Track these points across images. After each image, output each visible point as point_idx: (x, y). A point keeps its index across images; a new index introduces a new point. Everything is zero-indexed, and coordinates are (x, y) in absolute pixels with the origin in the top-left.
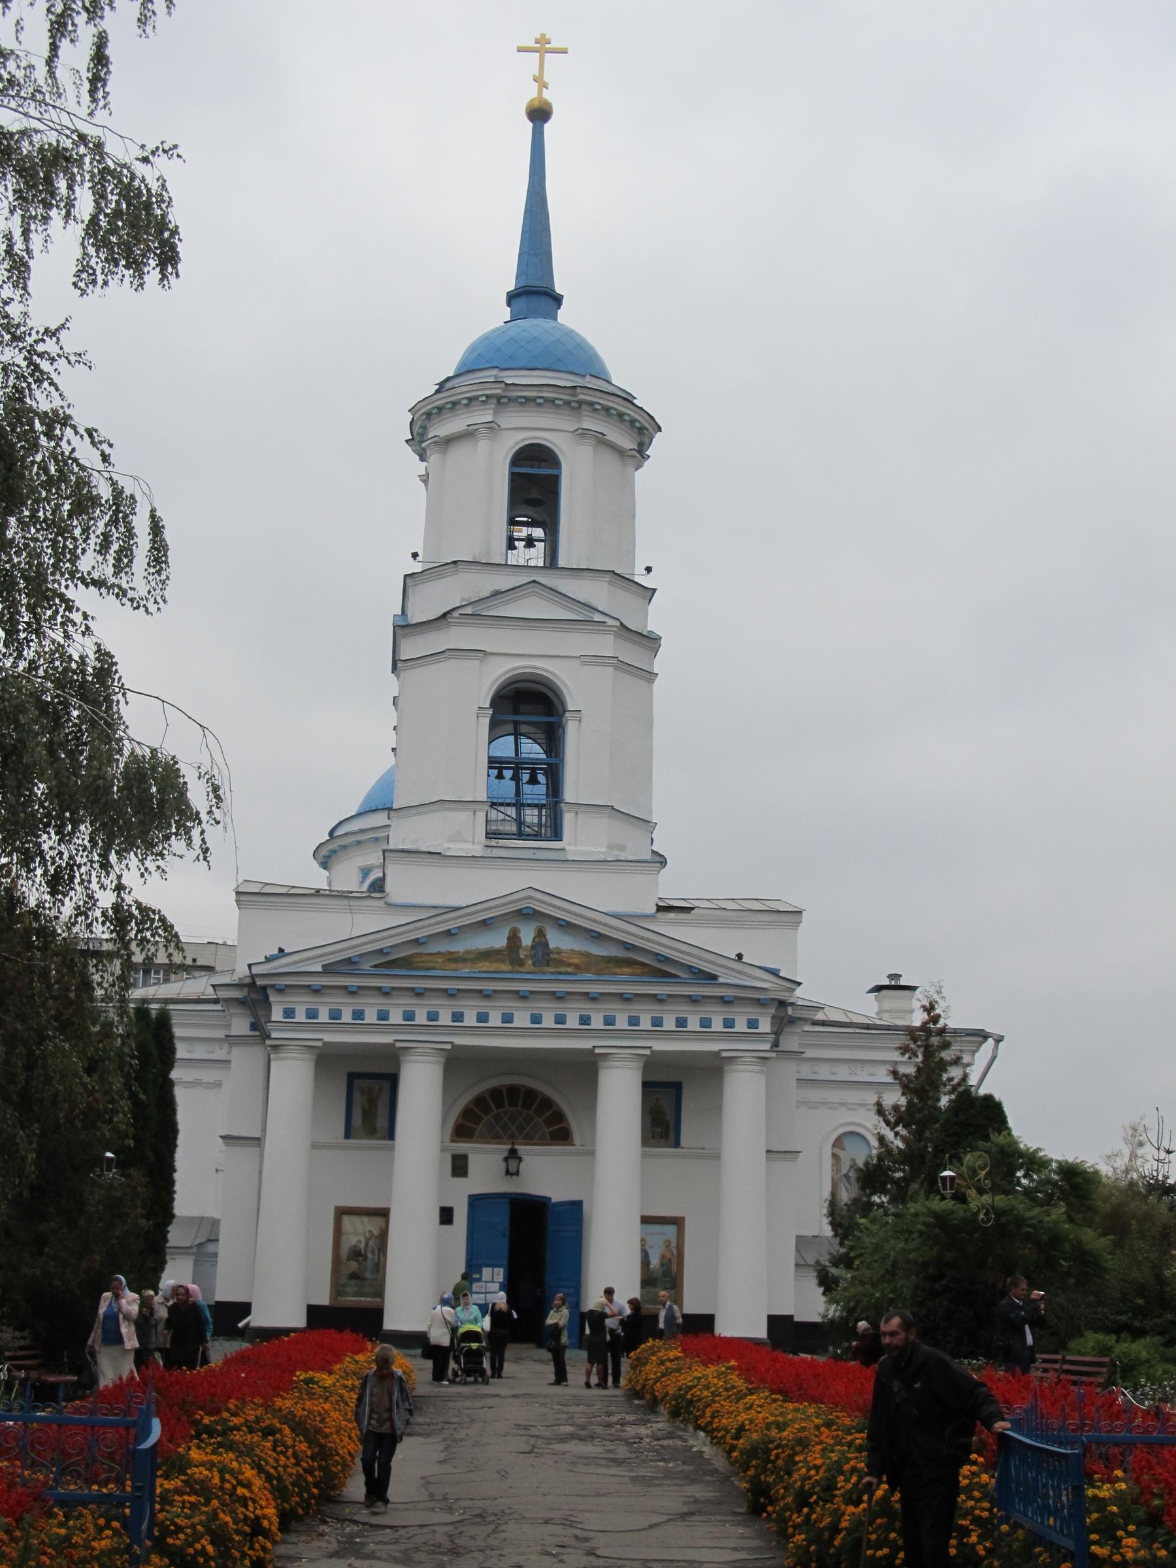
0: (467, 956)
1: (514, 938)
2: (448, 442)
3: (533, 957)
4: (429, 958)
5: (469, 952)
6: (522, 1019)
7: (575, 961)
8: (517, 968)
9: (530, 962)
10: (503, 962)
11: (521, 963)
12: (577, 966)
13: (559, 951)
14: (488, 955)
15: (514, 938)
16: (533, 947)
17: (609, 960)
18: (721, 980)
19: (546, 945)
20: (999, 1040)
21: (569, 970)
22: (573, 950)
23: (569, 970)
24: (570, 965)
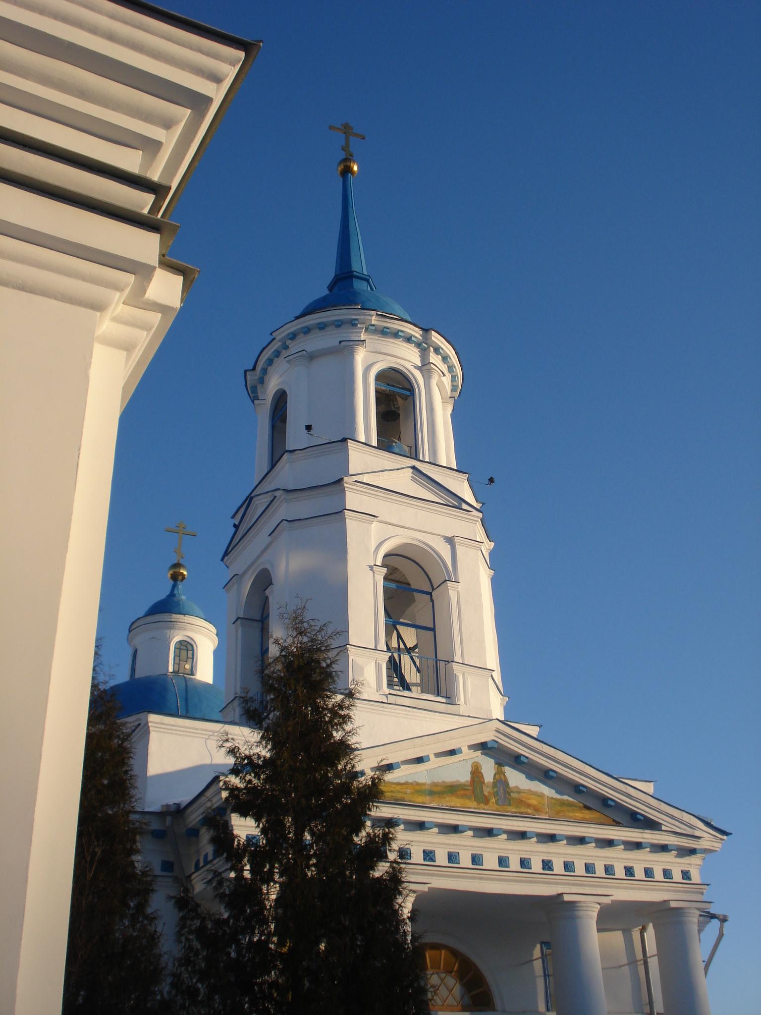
0: (435, 789)
1: (476, 773)
2: (312, 357)
3: (496, 794)
4: (398, 788)
5: (435, 784)
6: (490, 861)
7: (534, 802)
8: (482, 805)
9: (493, 800)
10: (469, 798)
11: (487, 802)
12: (537, 809)
13: (519, 791)
14: (452, 789)
15: (476, 773)
16: (495, 784)
17: (563, 803)
18: (664, 828)
19: (505, 783)
20: (724, 920)
21: (529, 811)
22: (530, 790)
23: (529, 811)
24: (529, 806)
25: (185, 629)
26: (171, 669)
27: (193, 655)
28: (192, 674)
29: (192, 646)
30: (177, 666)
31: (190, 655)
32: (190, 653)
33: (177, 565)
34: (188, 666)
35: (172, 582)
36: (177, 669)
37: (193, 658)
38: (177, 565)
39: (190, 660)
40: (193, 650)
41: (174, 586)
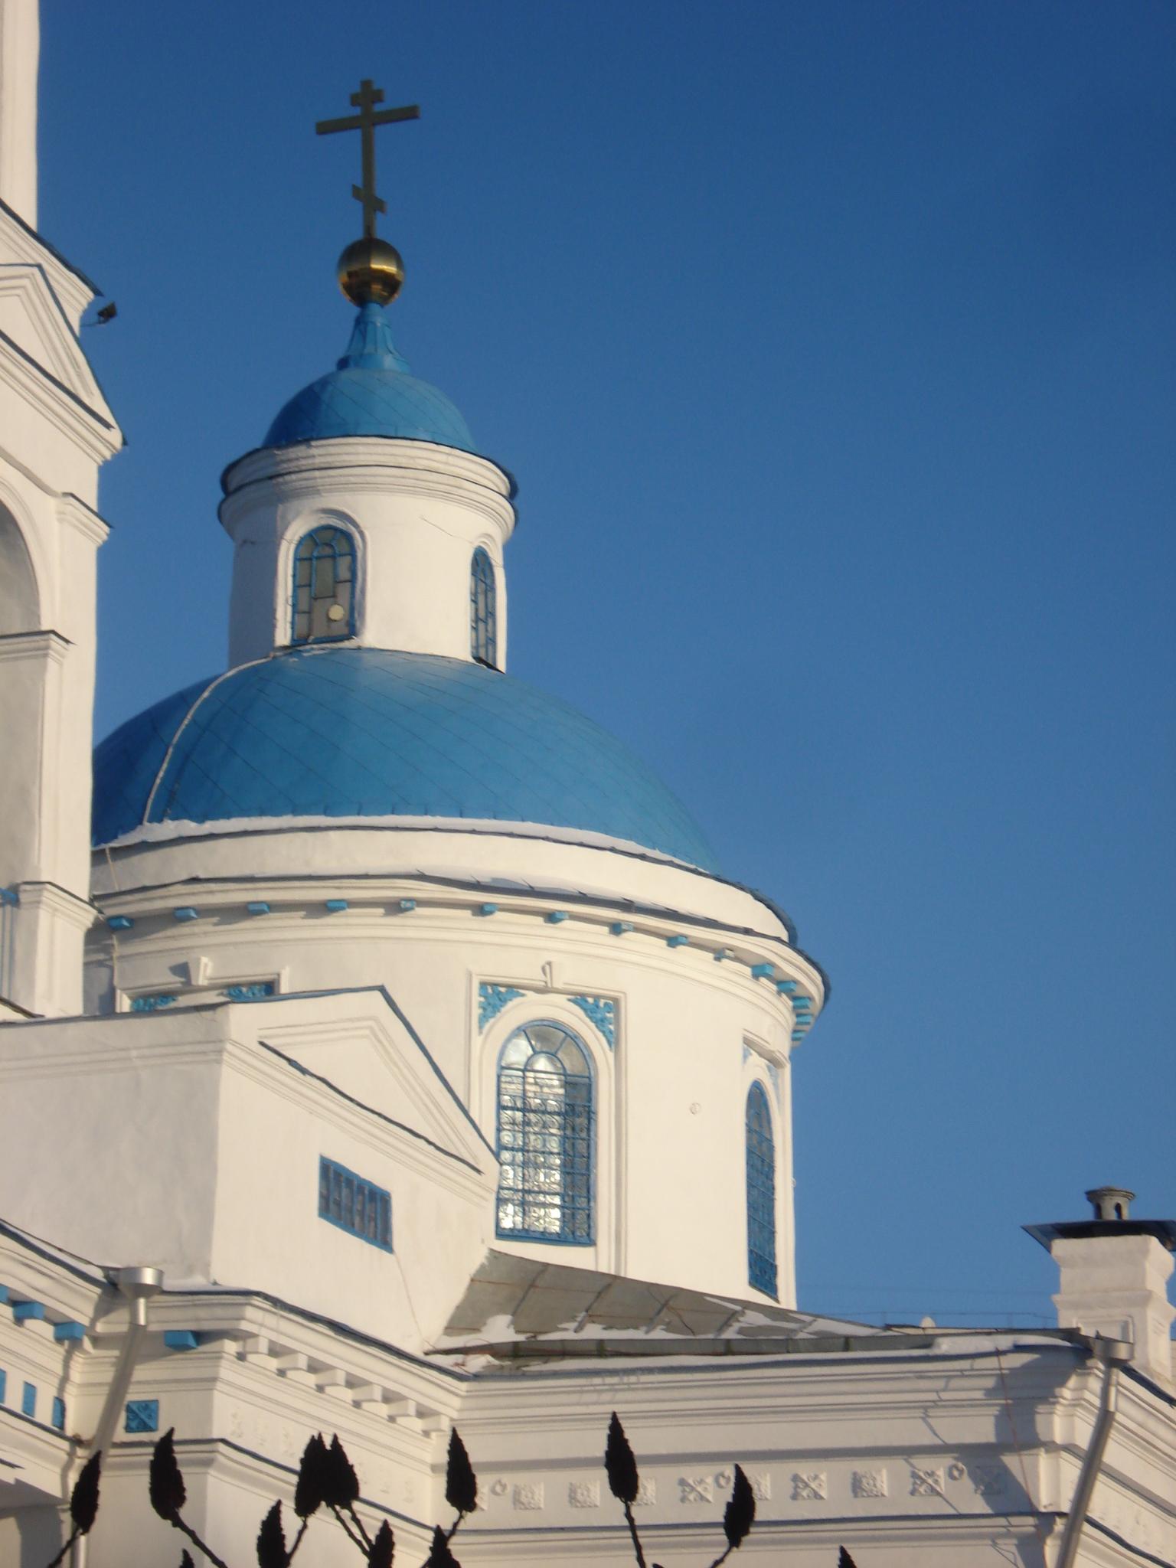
25: (313, 491)
26: (283, 636)
27: (353, 571)
28: (352, 629)
29: (348, 537)
30: (302, 620)
31: (344, 573)
32: (344, 563)
33: (369, 245)
34: (337, 612)
35: (355, 310)
36: (303, 629)
37: (353, 580)
38: (369, 245)
39: (343, 591)
40: (352, 553)
41: (361, 323)
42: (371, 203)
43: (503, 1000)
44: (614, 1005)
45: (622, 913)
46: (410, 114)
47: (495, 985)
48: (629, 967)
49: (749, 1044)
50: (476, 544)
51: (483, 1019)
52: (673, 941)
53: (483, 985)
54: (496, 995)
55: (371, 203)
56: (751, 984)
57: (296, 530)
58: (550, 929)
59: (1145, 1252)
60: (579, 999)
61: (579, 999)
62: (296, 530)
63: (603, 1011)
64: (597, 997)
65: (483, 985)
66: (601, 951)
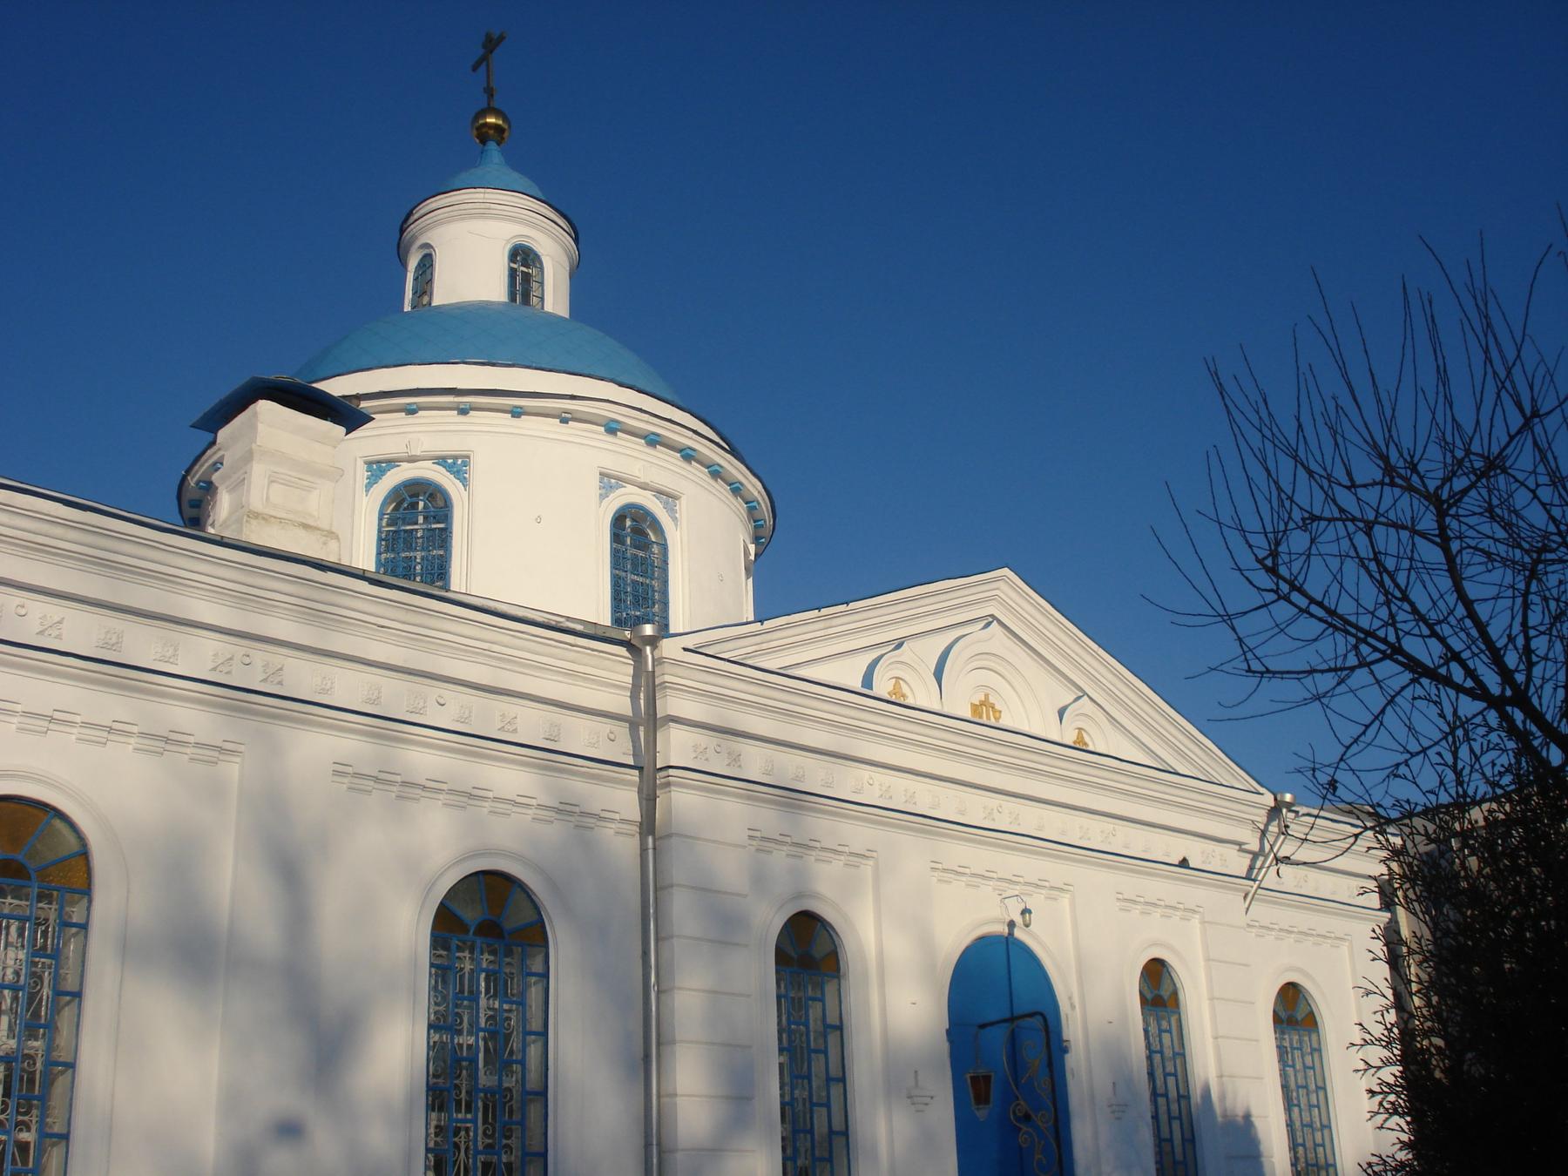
25: (414, 238)
42: (489, 92)
43: (383, 472)
44: (466, 460)
45: (462, 400)
46: (502, 38)
47: (379, 462)
48: (481, 436)
49: (609, 481)
50: (517, 241)
51: (369, 486)
52: (517, 413)
53: (369, 463)
54: (378, 468)
55: (489, 92)
56: (610, 438)
57: (413, 263)
58: (411, 419)
59: (255, 414)
60: (441, 460)
61: (441, 460)
62: (413, 263)
63: (457, 465)
64: (456, 458)
65: (369, 463)
66: (452, 428)
